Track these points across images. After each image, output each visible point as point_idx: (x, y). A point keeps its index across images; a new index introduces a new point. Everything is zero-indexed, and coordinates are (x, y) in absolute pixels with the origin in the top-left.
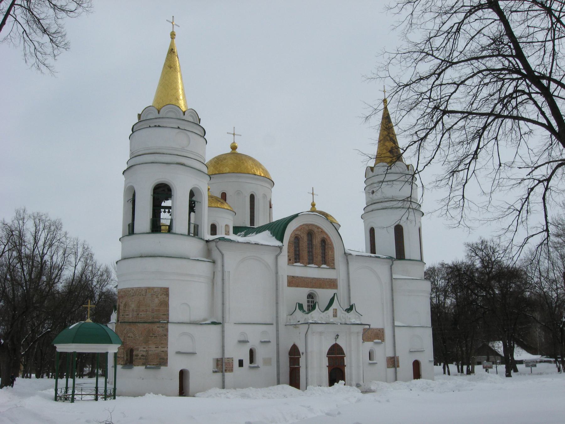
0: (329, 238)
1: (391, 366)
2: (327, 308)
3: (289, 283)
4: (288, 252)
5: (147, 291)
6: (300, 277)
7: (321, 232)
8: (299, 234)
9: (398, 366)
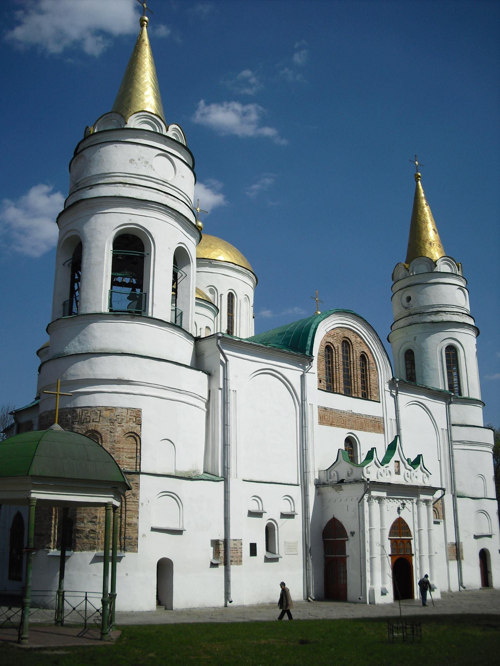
0: (371, 353)
2: (386, 461)
5: (104, 413)
7: (361, 342)
9: (463, 559)
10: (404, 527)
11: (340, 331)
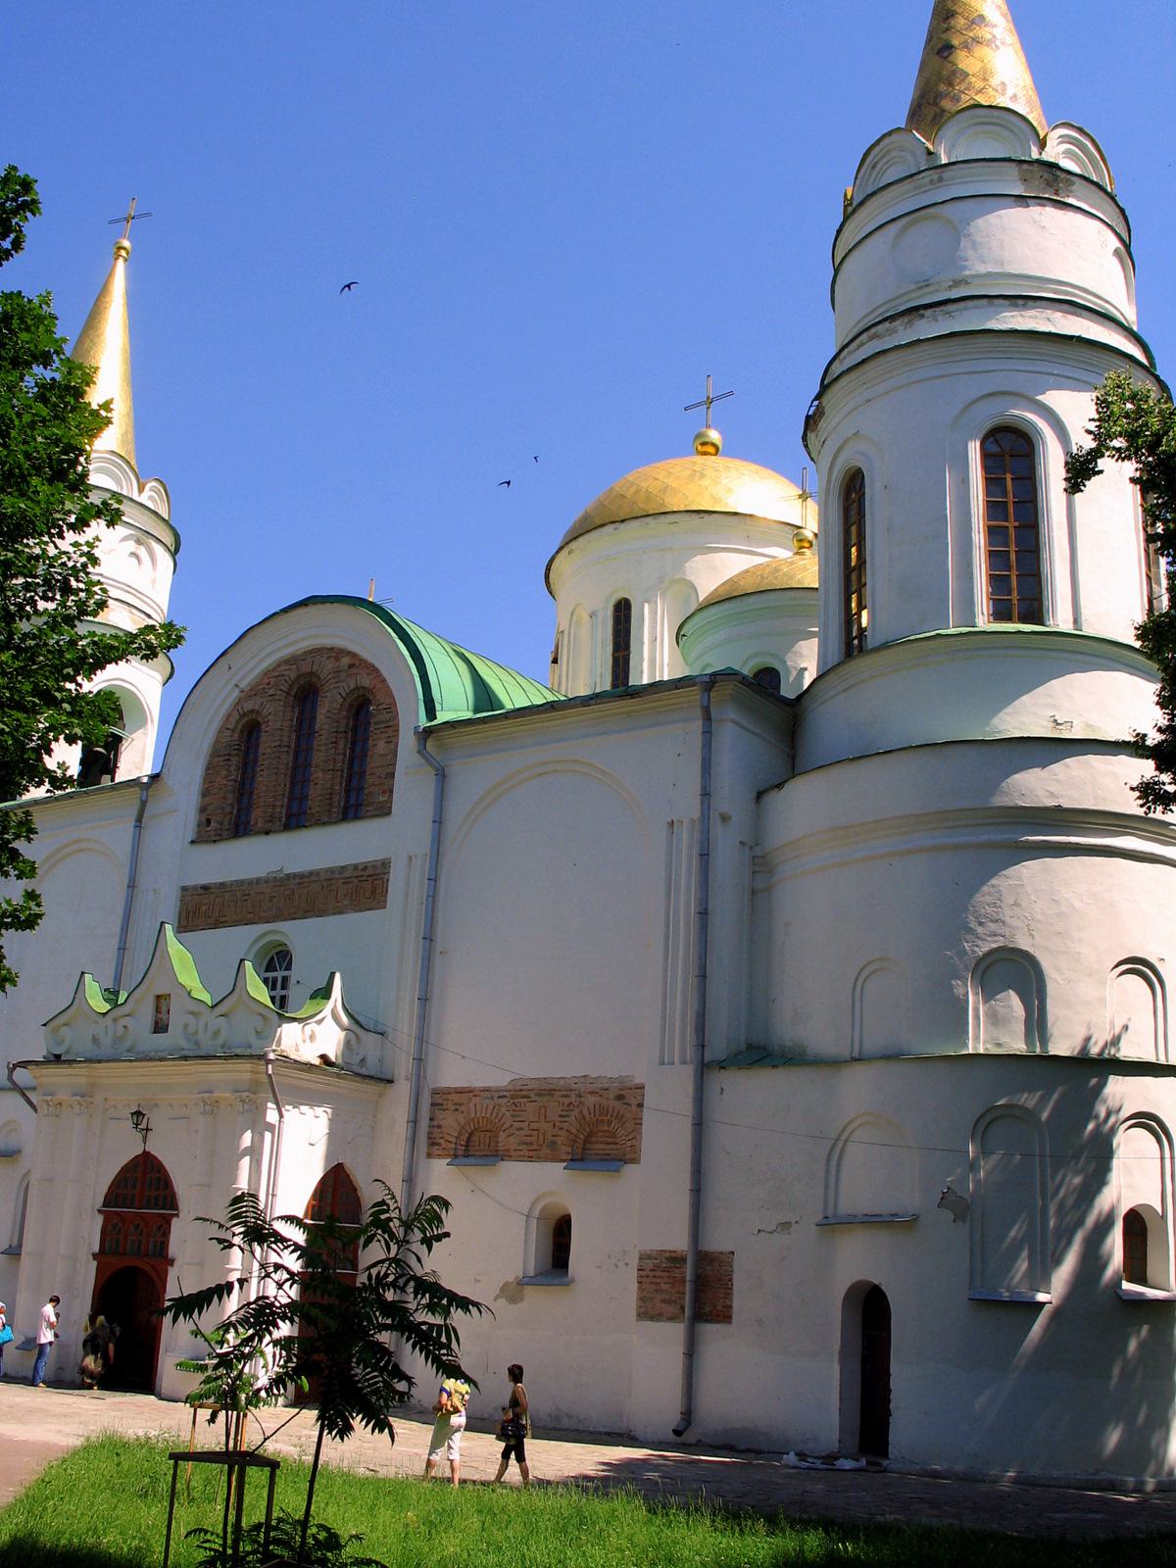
1: (671, 1309)
3: (187, 917)
4: (205, 793)
6: (232, 883)
7: (351, 666)
8: (257, 708)
9: (724, 1316)
10: (159, 1179)
11: (288, 667)
